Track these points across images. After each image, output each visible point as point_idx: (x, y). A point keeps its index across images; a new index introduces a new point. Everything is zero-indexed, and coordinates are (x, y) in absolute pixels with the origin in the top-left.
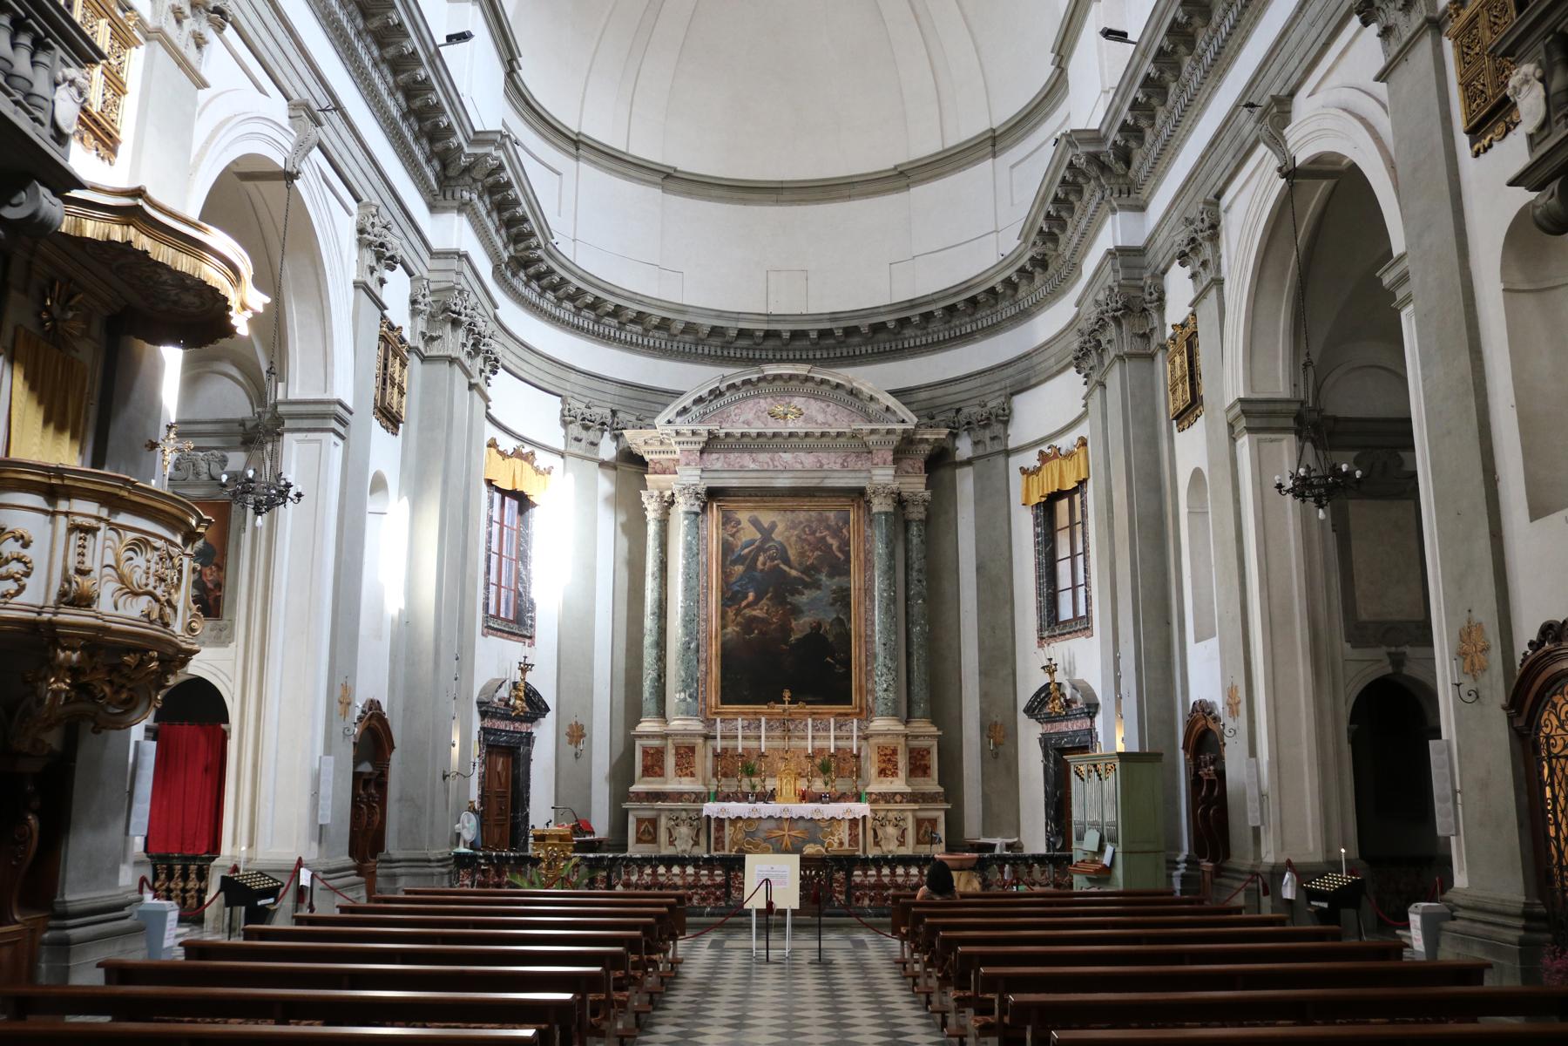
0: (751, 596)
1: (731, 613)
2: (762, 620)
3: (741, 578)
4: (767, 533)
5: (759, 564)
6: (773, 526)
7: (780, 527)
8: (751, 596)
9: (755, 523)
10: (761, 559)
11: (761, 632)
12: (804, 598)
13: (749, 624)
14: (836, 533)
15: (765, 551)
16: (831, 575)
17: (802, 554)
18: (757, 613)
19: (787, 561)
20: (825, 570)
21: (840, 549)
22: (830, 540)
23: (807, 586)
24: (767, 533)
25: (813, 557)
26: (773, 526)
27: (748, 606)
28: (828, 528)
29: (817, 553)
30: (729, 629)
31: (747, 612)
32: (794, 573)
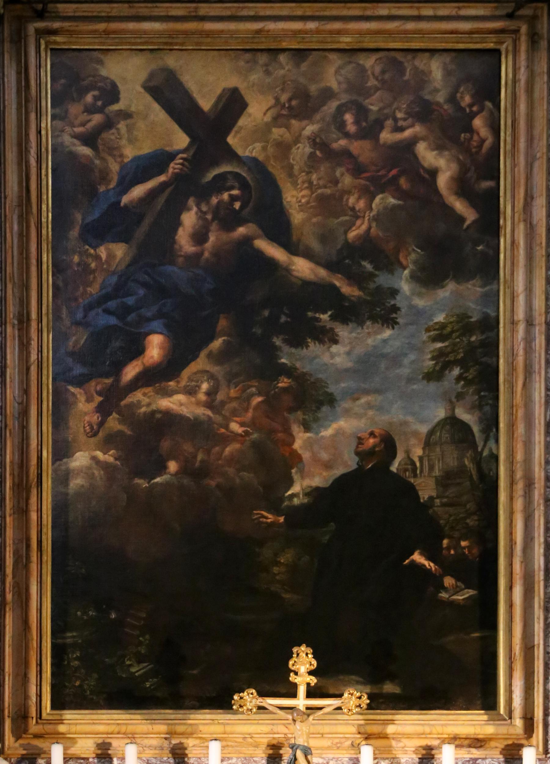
0: (155, 348)
1: (84, 406)
2: (194, 428)
3: (120, 289)
4: (211, 128)
5: (184, 239)
6: (233, 104)
7: (257, 111)
8: (155, 348)
9: (168, 92)
10: (189, 219)
11: (186, 470)
12: (335, 356)
13: (147, 440)
14: (452, 130)
15: (203, 194)
16: (430, 277)
17: (328, 205)
18: (176, 403)
19: (279, 229)
20: (411, 257)
21: (462, 187)
22: (427, 155)
23: (348, 312)
24: (211, 128)
25: (367, 215)
26: (233, 104)
27: (153, 377)
28: (424, 112)
29: (384, 200)
30: (80, 460)
31: (145, 400)
32: (302, 267)
